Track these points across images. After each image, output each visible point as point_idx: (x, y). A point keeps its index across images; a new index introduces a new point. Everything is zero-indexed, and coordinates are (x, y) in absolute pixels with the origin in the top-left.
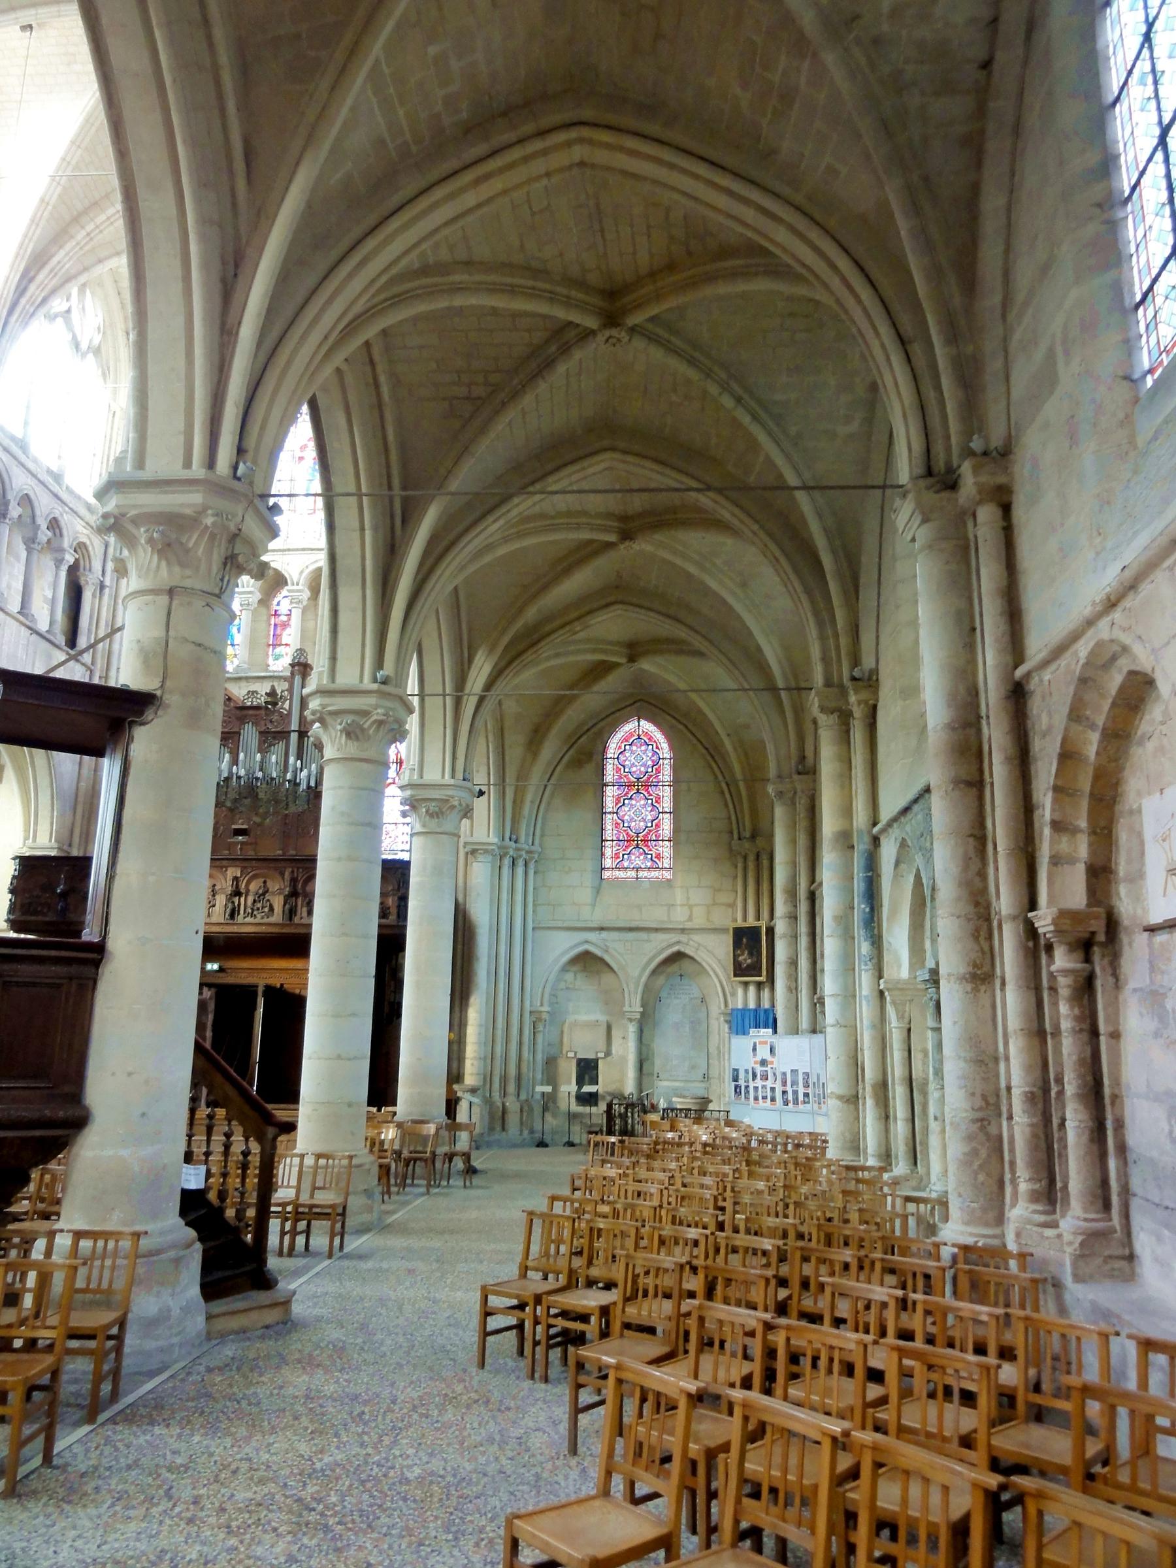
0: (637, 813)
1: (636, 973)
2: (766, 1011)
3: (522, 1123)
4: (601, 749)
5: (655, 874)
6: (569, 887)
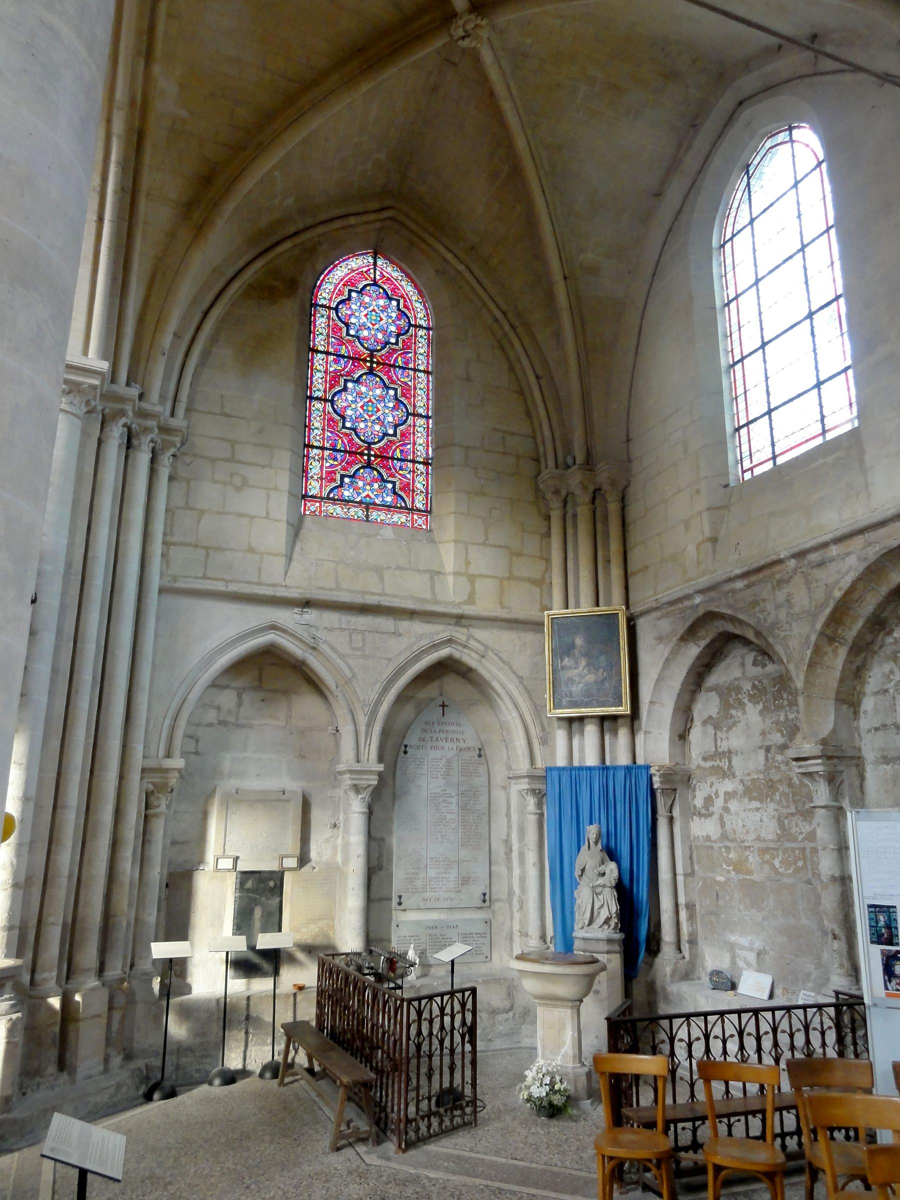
0: (367, 407)
1: (373, 696)
2: (628, 769)
3: (108, 1042)
4: (309, 282)
5: (400, 518)
6: (240, 515)
